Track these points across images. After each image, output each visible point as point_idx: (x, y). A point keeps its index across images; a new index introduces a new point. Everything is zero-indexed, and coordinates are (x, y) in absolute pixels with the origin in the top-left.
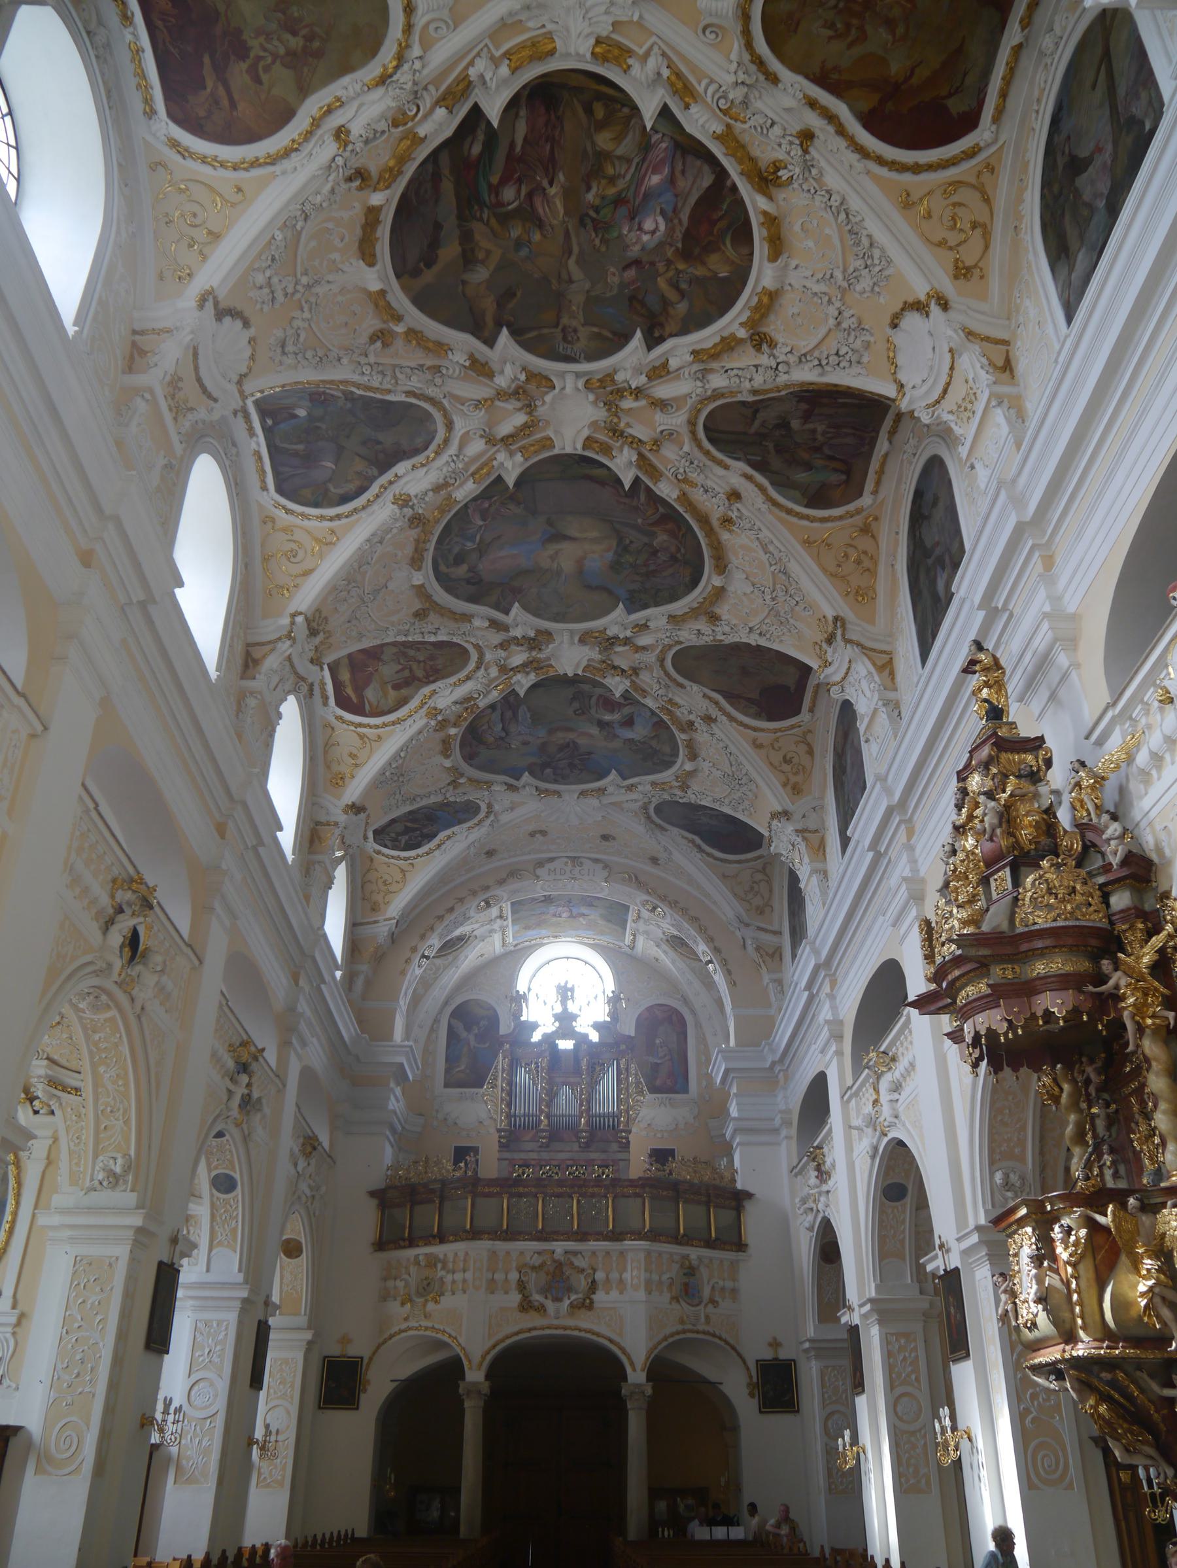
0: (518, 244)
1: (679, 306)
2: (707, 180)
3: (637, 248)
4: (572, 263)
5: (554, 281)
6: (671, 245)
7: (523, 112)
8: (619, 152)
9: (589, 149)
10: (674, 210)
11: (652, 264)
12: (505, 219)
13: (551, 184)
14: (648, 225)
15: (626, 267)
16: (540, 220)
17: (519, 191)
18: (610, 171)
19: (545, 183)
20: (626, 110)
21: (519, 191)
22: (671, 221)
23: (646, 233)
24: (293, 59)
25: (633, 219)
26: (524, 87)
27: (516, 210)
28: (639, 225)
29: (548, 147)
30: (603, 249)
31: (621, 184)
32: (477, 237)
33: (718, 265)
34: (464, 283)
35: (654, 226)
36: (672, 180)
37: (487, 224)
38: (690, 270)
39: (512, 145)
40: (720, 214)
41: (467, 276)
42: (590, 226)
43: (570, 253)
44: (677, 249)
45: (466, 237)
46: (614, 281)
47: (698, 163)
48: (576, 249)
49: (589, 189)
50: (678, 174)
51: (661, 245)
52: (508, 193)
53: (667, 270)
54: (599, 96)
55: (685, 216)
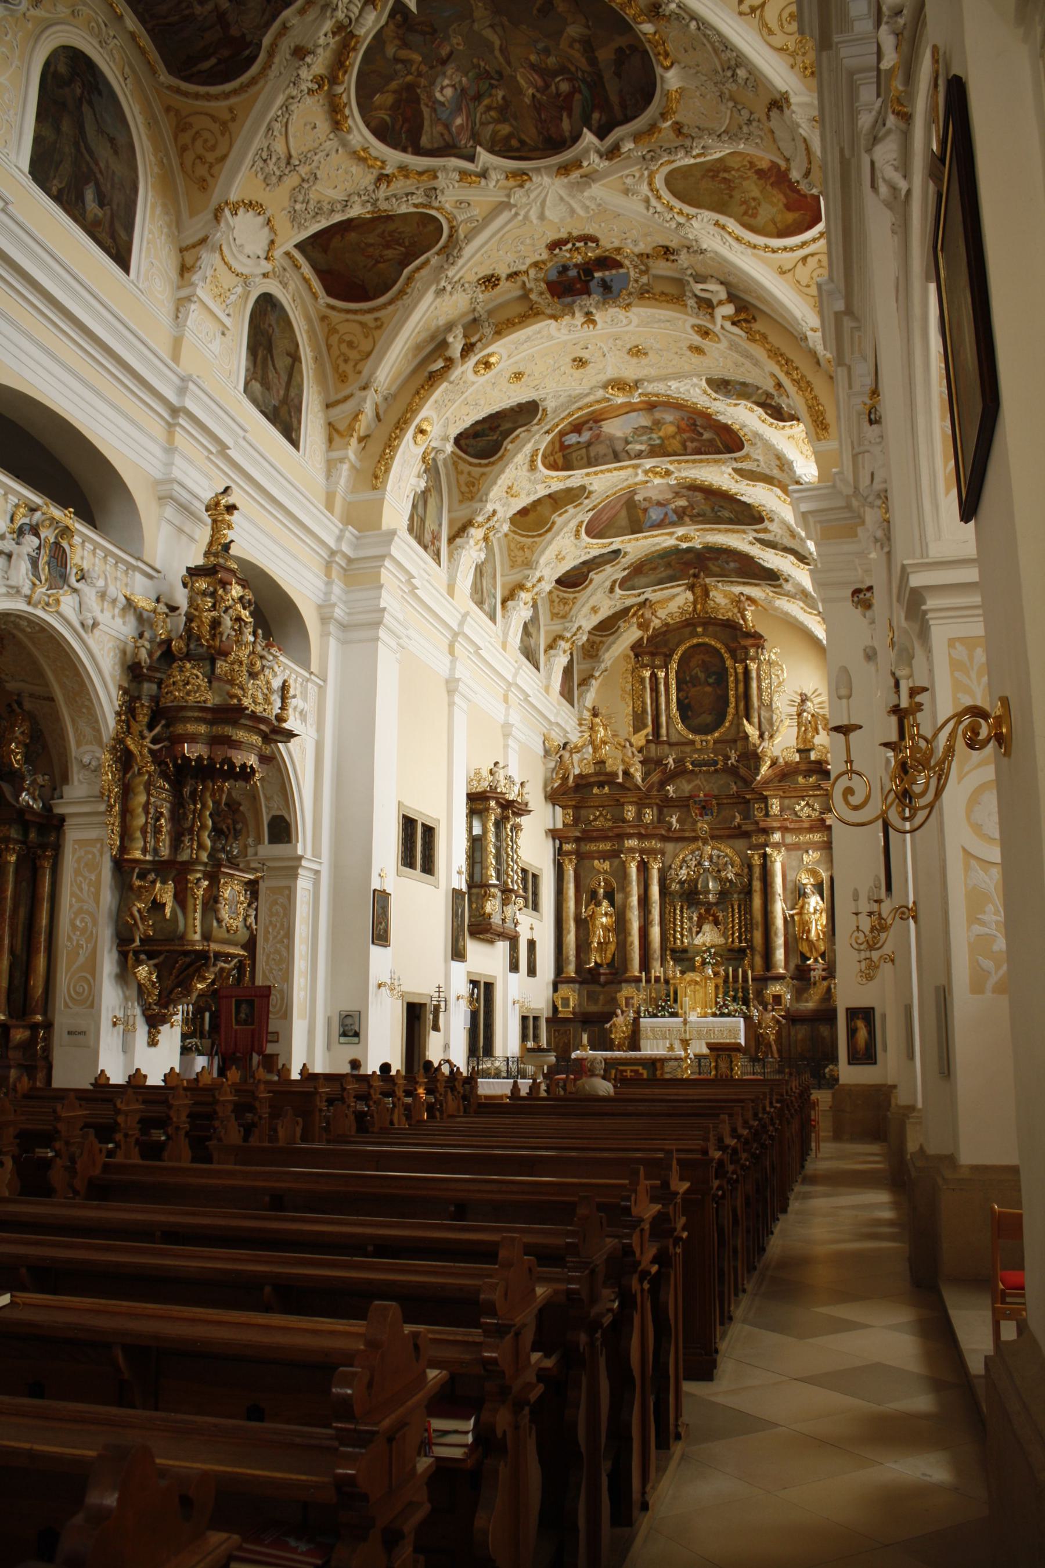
0: (547, 51)
1: (393, 51)
2: (424, 141)
3: (449, 72)
4: (497, 43)
5: (507, 23)
6: (425, 87)
7: (567, 134)
8: (491, 127)
9: (514, 122)
10: (435, 110)
11: (432, 67)
12: (562, 70)
13: (533, 96)
14: (449, 92)
15: (451, 53)
16: (534, 70)
17: (557, 88)
18: (492, 113)
19: (538, 95)
20: (497, 149)
21: (557, 88)
22: (434, 103)
23: (448, 85)
24: (727, 170)
25: (462, 90)
26: (570, 147)
27: (556, 76)
28: (456, 89)
29: (543, 117)
30: (475, 61)
31: (481, 108)
32: (583, 60)
33: (383, 99)
34: (588, 27)
35: (445, 92)
36: (447, 126)
37: (577, 68)
38: (400, 81)
39: (570, 116)
40: (404, 129)
41: (587, 32)
42: (493, 73)
43: (501, 50)
44: (419, 87)
45: (593, 61)
46: (456, 40)
47: (436, 146)
48: (497, 53)
49: (504, 98)
50: (445, 132)
51: (433, 83)
52: (565, 87)
53: (418, 68)
54: (518, 150)
55: (426, 111)
